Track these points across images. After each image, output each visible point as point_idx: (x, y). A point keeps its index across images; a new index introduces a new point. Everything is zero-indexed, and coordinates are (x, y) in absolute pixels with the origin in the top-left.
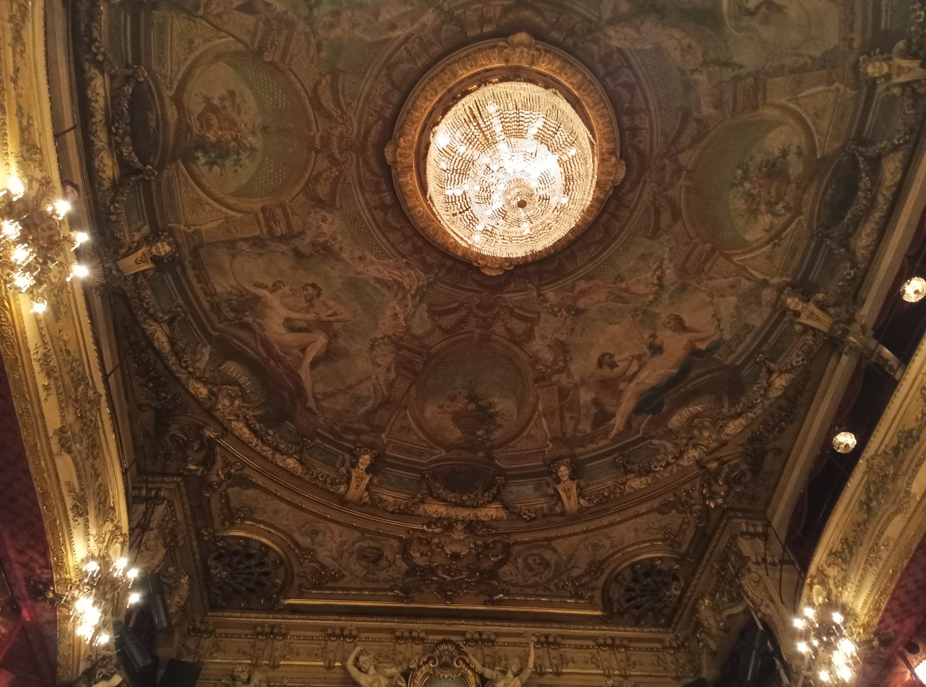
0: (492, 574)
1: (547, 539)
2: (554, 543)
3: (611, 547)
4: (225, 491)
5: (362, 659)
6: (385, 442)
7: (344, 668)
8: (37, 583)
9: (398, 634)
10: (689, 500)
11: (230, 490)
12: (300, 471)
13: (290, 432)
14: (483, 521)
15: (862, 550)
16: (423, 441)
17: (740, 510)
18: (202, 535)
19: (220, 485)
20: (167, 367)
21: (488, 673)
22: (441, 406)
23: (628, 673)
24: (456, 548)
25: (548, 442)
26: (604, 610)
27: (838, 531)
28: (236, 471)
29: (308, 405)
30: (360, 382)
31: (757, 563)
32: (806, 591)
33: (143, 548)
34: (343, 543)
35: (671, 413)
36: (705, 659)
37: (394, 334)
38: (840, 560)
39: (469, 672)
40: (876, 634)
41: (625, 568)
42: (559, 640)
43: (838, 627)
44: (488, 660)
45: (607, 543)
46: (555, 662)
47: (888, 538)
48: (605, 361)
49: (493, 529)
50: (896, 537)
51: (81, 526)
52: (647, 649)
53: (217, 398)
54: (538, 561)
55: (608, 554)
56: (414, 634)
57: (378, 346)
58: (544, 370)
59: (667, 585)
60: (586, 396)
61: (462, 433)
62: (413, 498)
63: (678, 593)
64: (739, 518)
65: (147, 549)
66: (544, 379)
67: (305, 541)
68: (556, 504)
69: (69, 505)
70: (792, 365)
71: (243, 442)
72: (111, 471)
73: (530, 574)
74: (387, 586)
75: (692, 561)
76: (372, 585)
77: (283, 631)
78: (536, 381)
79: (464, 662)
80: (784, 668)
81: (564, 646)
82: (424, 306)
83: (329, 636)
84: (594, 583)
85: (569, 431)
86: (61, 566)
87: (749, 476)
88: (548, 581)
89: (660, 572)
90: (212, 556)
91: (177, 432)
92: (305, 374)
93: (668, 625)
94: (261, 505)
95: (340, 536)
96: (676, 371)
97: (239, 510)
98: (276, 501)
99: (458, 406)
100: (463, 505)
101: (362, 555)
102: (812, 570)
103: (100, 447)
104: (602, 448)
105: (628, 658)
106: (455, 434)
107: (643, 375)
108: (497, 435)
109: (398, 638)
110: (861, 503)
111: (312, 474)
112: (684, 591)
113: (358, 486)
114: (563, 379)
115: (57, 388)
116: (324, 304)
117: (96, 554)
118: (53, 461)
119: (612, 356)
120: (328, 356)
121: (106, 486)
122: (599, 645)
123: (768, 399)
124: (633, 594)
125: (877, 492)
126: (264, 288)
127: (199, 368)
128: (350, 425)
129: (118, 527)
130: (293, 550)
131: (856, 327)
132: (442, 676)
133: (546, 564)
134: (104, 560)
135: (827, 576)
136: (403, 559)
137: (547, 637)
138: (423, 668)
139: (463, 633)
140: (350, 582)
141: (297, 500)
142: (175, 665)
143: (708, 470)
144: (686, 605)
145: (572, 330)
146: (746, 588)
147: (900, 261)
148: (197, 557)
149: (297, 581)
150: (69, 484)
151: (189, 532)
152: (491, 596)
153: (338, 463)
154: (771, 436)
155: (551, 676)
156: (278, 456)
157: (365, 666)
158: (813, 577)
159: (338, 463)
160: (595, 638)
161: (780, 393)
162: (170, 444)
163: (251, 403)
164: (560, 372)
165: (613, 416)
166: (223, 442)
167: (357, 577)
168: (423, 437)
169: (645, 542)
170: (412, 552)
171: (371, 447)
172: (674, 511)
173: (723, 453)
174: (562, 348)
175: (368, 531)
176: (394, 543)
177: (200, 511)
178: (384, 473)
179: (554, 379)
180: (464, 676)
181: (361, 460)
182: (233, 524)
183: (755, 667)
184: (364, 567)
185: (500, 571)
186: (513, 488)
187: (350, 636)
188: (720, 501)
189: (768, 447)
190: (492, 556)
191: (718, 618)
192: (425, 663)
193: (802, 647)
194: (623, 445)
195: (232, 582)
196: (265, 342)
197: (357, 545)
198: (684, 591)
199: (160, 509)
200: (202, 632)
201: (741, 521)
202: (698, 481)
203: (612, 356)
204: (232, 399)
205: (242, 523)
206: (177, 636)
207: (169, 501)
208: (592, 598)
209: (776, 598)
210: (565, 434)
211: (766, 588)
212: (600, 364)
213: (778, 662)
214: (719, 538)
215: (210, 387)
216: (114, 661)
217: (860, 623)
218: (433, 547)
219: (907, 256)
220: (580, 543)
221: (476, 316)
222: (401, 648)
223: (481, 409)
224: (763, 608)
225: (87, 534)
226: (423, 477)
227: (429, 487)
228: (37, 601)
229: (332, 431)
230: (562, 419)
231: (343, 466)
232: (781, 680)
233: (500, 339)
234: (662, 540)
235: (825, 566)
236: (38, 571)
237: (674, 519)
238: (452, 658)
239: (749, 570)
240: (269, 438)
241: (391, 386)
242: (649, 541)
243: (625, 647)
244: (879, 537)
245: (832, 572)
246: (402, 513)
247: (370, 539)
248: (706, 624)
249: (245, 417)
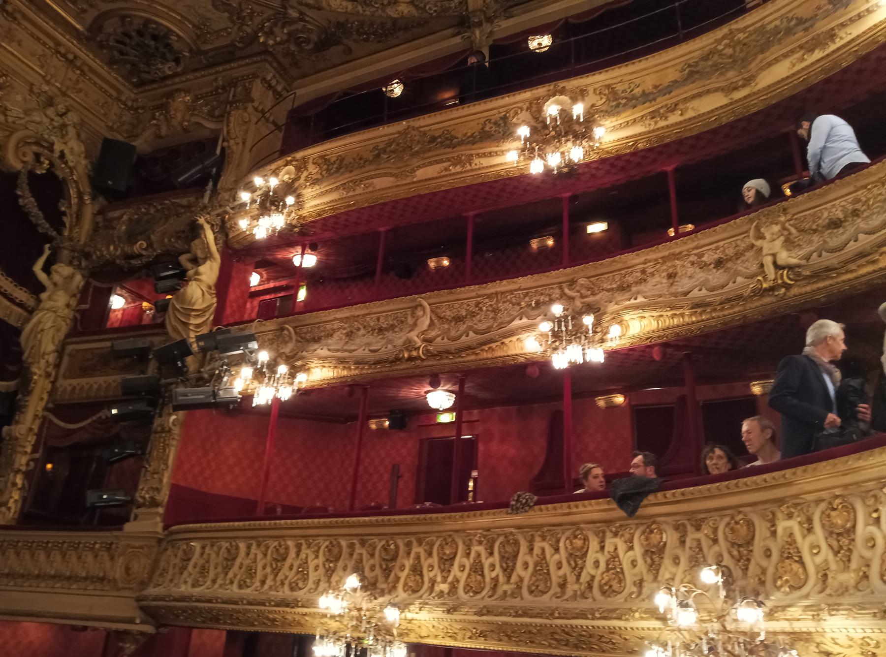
10: (247, 18)
15: (348, 175)
17: (278, 62)
23: (69, 93)
26: (89, 30)
27: (343, 149)
31: (256, 109)
32: (280, 162)
36: (147, 135)
38: (325, 167)
40: (302, 225)
41: (142, 17)
43: (284, 206)
47: (372, 183)
50: (378, 188)
52: (101, 88)
59: (165, 59)
63: (169, 73)
64: (273, 67)
70: (425, 6)
75: (204, 62)
80: (212, 191)
87: (311, 46)
89: (168, 46)
93: (136, 86)
102: (299, 155)
105: (77, 82)
110: (376, 148)
112: (176, 75)
122: (59, 52)
123: (383, 11)
124: (128, 41)
125: (393, 152)
131: (487, 27)
135: (306, 168)
143: (286, 13)
144: (166, 86)
146: (232, 119)
147: (558, 18)
154: (355, 37)
158: (294, 159)
161: (395, 16)
169: (179, 14)
172: (226, 15)
173: (310, 13)
183: (192, 176)
188: (271, 42)
189: (345, 41)
191: (187, 117)
193: (245, 196)
198: (176, 75)
201: (272, 70)
202: (271, 12)
209: (249, 144)
211: (247, 131)
213: (211, 184)
214: (243, 66)
217: (300, 213)
219: (567, 19)
224: (232, 142)
232: (203, 197)
234: (194, 26)
235: (311, 160)
237: (220, 20)
239: (246, 109)
242: (182, 16)
243: (82, 71)
244: (367, 178)
245: (312, 169)
248: (172, 112)
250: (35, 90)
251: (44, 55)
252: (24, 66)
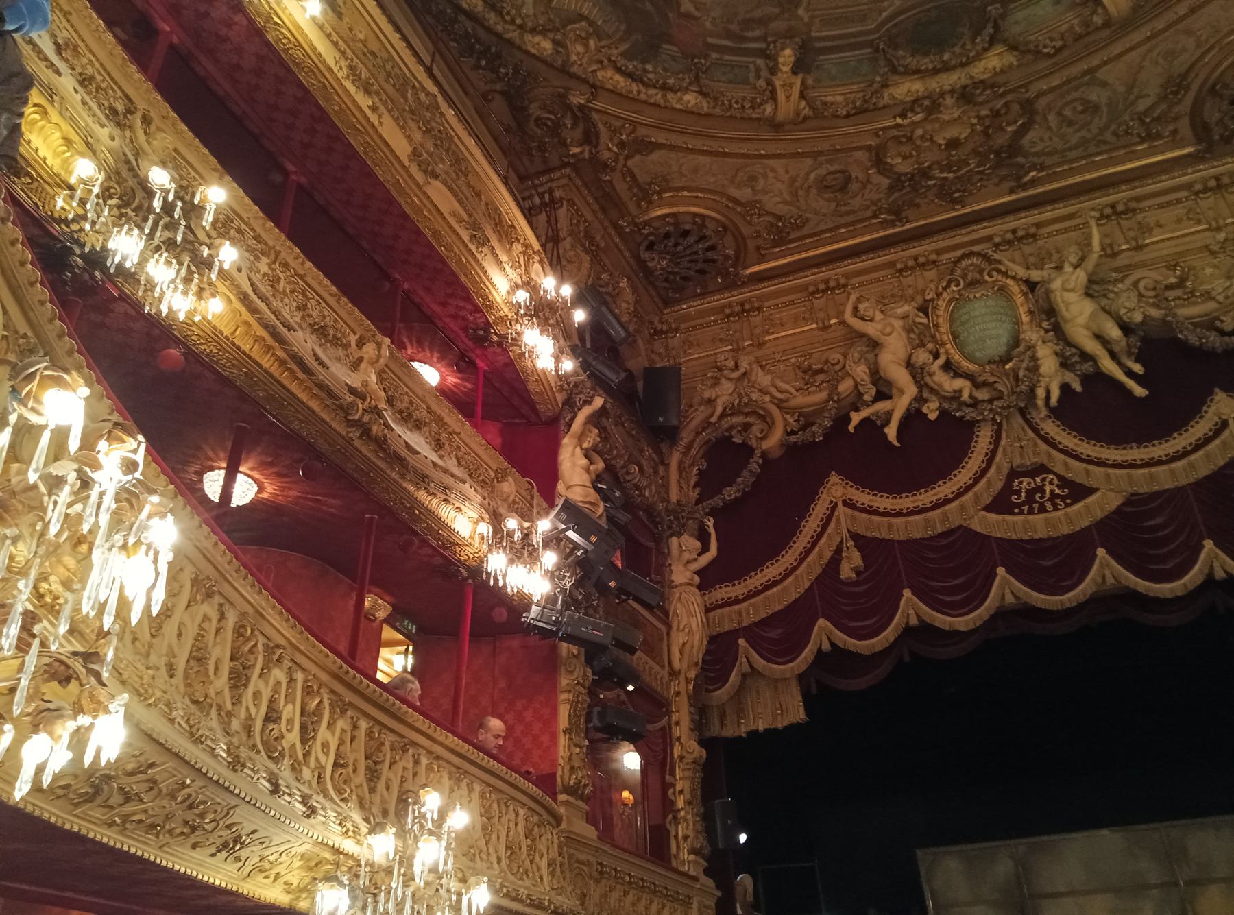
0: (1014, 148)
2: (1101, 74)
4: (625, 165)
5: (861, 307)
6: (806, 20)
7: (843, 323)
8: (475, 330)
9: (899, 266)
11: (630, 163)
12: (705, 106)
13: (673, 58)
14: (982, 82)
18: (622, 227)
19: (616, 160)
20: (489, 30)
21: (1035, 275)
24: (952, 132)
26: (1199, 141)
28: (628, 136)
29: (683, 9)
33: (564, 263)
34: (793, 180)
39: (1009, 281)
42: (1133, 205)
44: (1032, 260)
46: (1131, 234)
49: (1000, 87)
51: (489, 257)
53: (565, 47)
55: (1196, 56)
56: (922, 260)
62: (870, 86)
65: (569, 262)
67: (744, 194)
68: (1094, 12)
69: (466, 239)
71: (620, 95)
72: (490, 185)
73: (1070, 130)
74: (869, 213)
77: (756, 305)
79: (999, 271)
81: (1142, 210)
83: (813, 293)
84: (1176, 109)
86: (490, 305)
88: (1102, 131)
90: (642, 248)
91: (539, 113)
94: (675, 168)
95: (787, 172)
97: (650, 184)
98: (691, 156)
100: (947, 68)
101: (823, 186)
103: (465, 160)
109: (901, 271)
111: (723, 103)
113: (788, 97)
115: (385, 104)
117: (519, 282)
118: (425, 193)
121: (493, 203)
127: (527, 16)
129: (527, 246)
130: (734, 209)
132: (972, 296)
133: (1092, 108)
134: (530, 285)
136: (879, 172)
137: (1113, 206)
138: (945, 295)
139: (989, 239)
140: (817, 225)
141: (716, 146)
142: (651, 374)
148: (627, 254)
149: (751, 245)
150: (454, 214)
151: (605, 229)
152: (1019, 178)
153: (752, 76)
155: (1129, 253)
156: (670, 96)
157: (870, 313)
159: (752, 76)
160: (1188, 186)
162: (539, 131)
163: (609, 37)
166: (597, 104)
167: (824, 215)
170: (889, 160)
171: (789, 34)
175: (821, 153)
176: (861, 155)
177: (608, 201)
178: (818, 67)
180: (1003, 289)
181: (781, 60)
182: (650, 202)
184: (828, 200)
185: (1025, 141)
186: (1019, 15)
187: (838, 286)
190: (1009, 124)
192: (945, 289)
195: (676, 270)
197: (812, 176)
199: (563, 213)
200: (666, 333)
204: (584, 41)
205: (661, 198)
206: (640, 343)
207: (568, 201)
208: (1175, 131)
215: (551, 35)
216: (588, 385)
218: (919, 142)
220: (1143, 59)
222: (908, 280)
225: (499, 263)
226: (877, 50)
227: (889, 61)
228: (485, 348)
229: (729, 35)
231: (758, 77)
236: (471, 318)
238: (981, 272)
240: (650, 76)
246: (861, 111)
247: (828, 162)
249: (609, 60)
250: (1216, 248)
251: (1190, 210)
252: (1187, 239)
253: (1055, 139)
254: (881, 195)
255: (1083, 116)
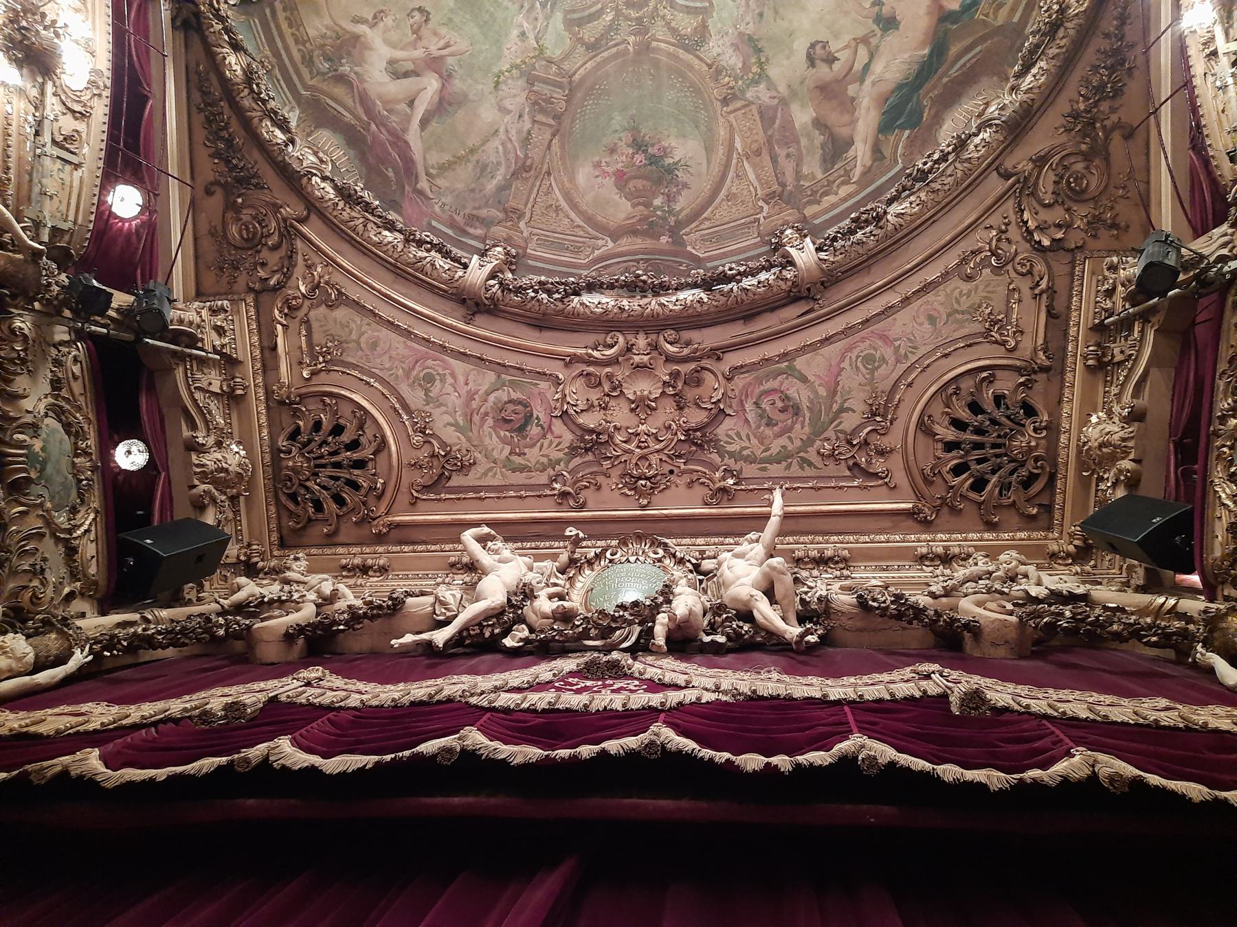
1: (784, 356)
2: (800, 363)
3: (898, 361)
6: (525, 234)
16: (579, 226)
22: (597, 165)
25: (761, 203)
29: (418, 186)
30: (485, 141)
34: (471, 396)
35: (937, 120)
37: (524, 63)
45: (888, 353)
48: (818, 55)
54: (780, 404)
55: (895, 376)
57: (505, 82)
58: (732, 84)
60: (802, 116)
61: (634, 206)
66: (735, 97)
73: (769, 432)
76: (520, 478)
78: (725, 101)
82: (559, 16)
85: (790, 179)
92: (414, 137)
94: (354, 337)
96: (926, 51)
99: (620, 161)
104: (845, 200)
106: (622, 210)
107: (878, 67)
108: (683, 203)
114: (760, 93)
116: (435, 34)
119: (825, 45)
120: (444, 105)
126: (362, 23)
128: (475, 212)
133: (792, 409)
140: (485, 474)
145: (761, 15)
164: (756, 82)
165: (850, 142)
168: (579, 222)
174: (752, 45)
179: (749, 95)
184: (504, 441)
194: (877, 189)
196: (364, 99)
202: (1009, 206)
203: (825, 45)
210: (783, 185)
212: (811, 60)
220: (842, 360)
221: (627, 18)
223: (653, 160)
229: (452, 224)
230: (774, 159)
233: (663, 45)
241: (526, 140)
253: (754, 441)
254: (561, 455)
255: (782, 416)
